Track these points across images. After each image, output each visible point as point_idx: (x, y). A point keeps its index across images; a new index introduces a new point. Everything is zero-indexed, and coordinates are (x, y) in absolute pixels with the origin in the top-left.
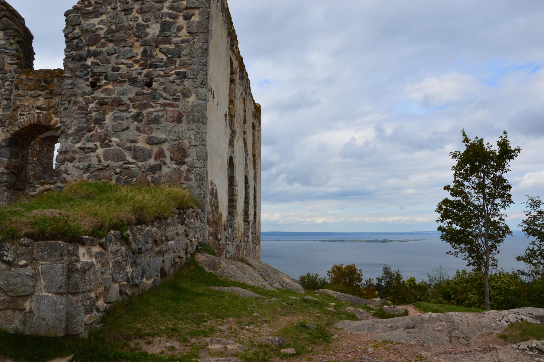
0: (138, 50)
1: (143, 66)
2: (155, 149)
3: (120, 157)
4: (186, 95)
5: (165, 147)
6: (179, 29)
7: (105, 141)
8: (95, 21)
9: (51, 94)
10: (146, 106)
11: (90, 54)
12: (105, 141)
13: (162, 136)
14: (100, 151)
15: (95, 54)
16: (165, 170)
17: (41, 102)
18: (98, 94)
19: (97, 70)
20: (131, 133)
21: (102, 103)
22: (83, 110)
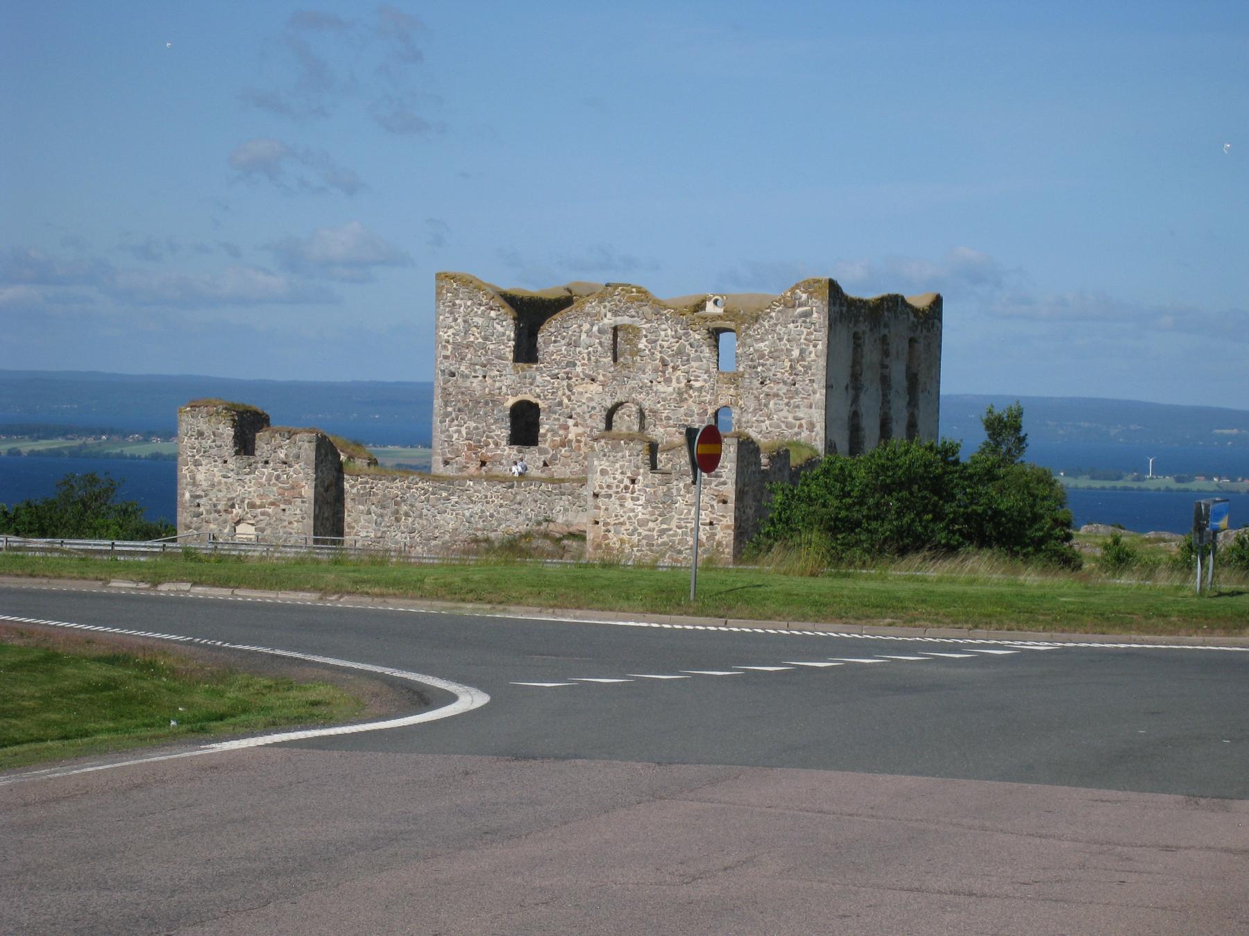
2: (798, 423)
3: (779, 427)
4: (814, 393)
5: (803, 422)
7: (769, 417)
8: (762, 345)
9: (737, 388)
10: (792, 398)
11: (759, 364)
12: (769, 417)
13: (801, 415)
14: (767, 422)
16: (803, 435)
18: (765, 389)
20: (784, 413)
21: (767, 395)
22: (757, 398)
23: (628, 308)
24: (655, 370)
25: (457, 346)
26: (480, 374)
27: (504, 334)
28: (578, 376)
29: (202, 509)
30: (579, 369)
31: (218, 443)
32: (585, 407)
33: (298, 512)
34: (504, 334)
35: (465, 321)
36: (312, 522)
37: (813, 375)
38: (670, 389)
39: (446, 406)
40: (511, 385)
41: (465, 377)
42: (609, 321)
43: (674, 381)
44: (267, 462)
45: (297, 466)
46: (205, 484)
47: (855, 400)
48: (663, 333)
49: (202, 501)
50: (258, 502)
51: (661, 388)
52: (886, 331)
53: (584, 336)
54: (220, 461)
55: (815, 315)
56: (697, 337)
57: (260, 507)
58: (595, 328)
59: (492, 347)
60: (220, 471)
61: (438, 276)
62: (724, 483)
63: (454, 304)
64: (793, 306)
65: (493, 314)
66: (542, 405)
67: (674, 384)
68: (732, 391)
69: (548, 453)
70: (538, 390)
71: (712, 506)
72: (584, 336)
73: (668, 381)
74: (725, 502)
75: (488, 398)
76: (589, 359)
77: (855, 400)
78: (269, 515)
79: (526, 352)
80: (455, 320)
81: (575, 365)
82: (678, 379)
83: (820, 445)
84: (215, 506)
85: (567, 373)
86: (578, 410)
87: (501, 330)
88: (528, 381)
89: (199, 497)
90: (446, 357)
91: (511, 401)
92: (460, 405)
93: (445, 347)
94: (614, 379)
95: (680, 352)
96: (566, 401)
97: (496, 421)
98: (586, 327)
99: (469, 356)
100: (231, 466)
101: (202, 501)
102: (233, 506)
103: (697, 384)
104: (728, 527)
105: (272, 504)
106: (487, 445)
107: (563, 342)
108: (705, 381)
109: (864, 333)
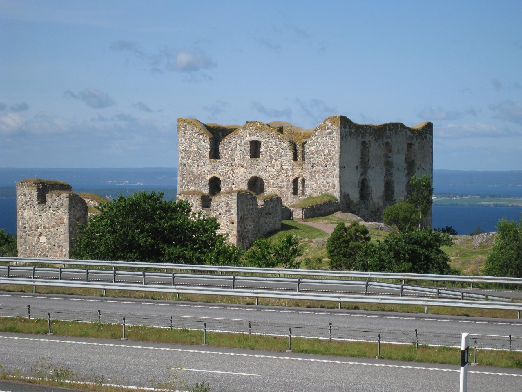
0: (323, 157)
1: (325, 162)
3: (320, 187)
4: (335, 170)
5: (330, 184)
6: (333, 151)
7: (316, 182)
8: (312, 148)
10: (325, 173)
12: (316, 182)
13: (330, 181)
14: (315, 185)
15: (313, 158)
16: (330, 190)
17: (300, 170)
18: (314, 169)
19: (314, 162)
20: (322, 180)
21: (315, 172)
23: (256, 132)
24: (268, 161)
26: (196, 165)
27: (205, 146)
28: (236, 165)
29: (26, 229)
30: (236, 161)
31: (32, 199)
32: (239, 179)
33: (63, 230)
34: (205, 146)
35: (190, 141)
36: (68, 235)
37: (334, 162)
38: (274, 170)
39: (183, 180)
40: (208, 169)
41: (191, 166)
42: (249, 139)
43: (276, 166)
44: (50, 207)
45: (62, 209)
46: (27, 218)
47: (364, 173)
48: (270, 144)
49: (26, 226)
50: (47, 226)
51: (270, 169)
52: (389, 140)
53: (238, 146)
54: (32, 207)
55: (334, 133)
56: (285, 145)
57: (49, 228)
58: (243, 142)
59: (201, 152)
60: (33, 212)
61: (178, 120)
62: (232, 214)
63: (185, 133)
64: (325, 129)
65: (201, 137)
66: (221, 179)
67: (276, 167)
68: (300, 170)
70: (220, 172)
71: (227, 225)
72: (238, 146)
73: (273, 166)
74: (233, 223)
76: (240, 157)
77: (364, 173)
78: (51, 232)
79: (215, 154)
80: (186, 140)
81: (235, 160)
82: (277, 165)
83: (337, 195)
84: (31, 228)
85: (232, 163)
86: (236, 181)
87: (204, 144)
88: (215, 167)
89: (25, 224)
90: (182, 157)
91: (209, 177)
92: (188, 179)
93: (182, 153)
94: (251, 166)
95: (278, 153)
96: (231, 176)
98: (239, 142)
100: (37, 209)
101: (26, 226)
102: (38, 228)
103: (285, 167)
104: (234, 235)
105: (53, 227)
107: (229, 149)
108: (288, 165)
109: (370, 141)
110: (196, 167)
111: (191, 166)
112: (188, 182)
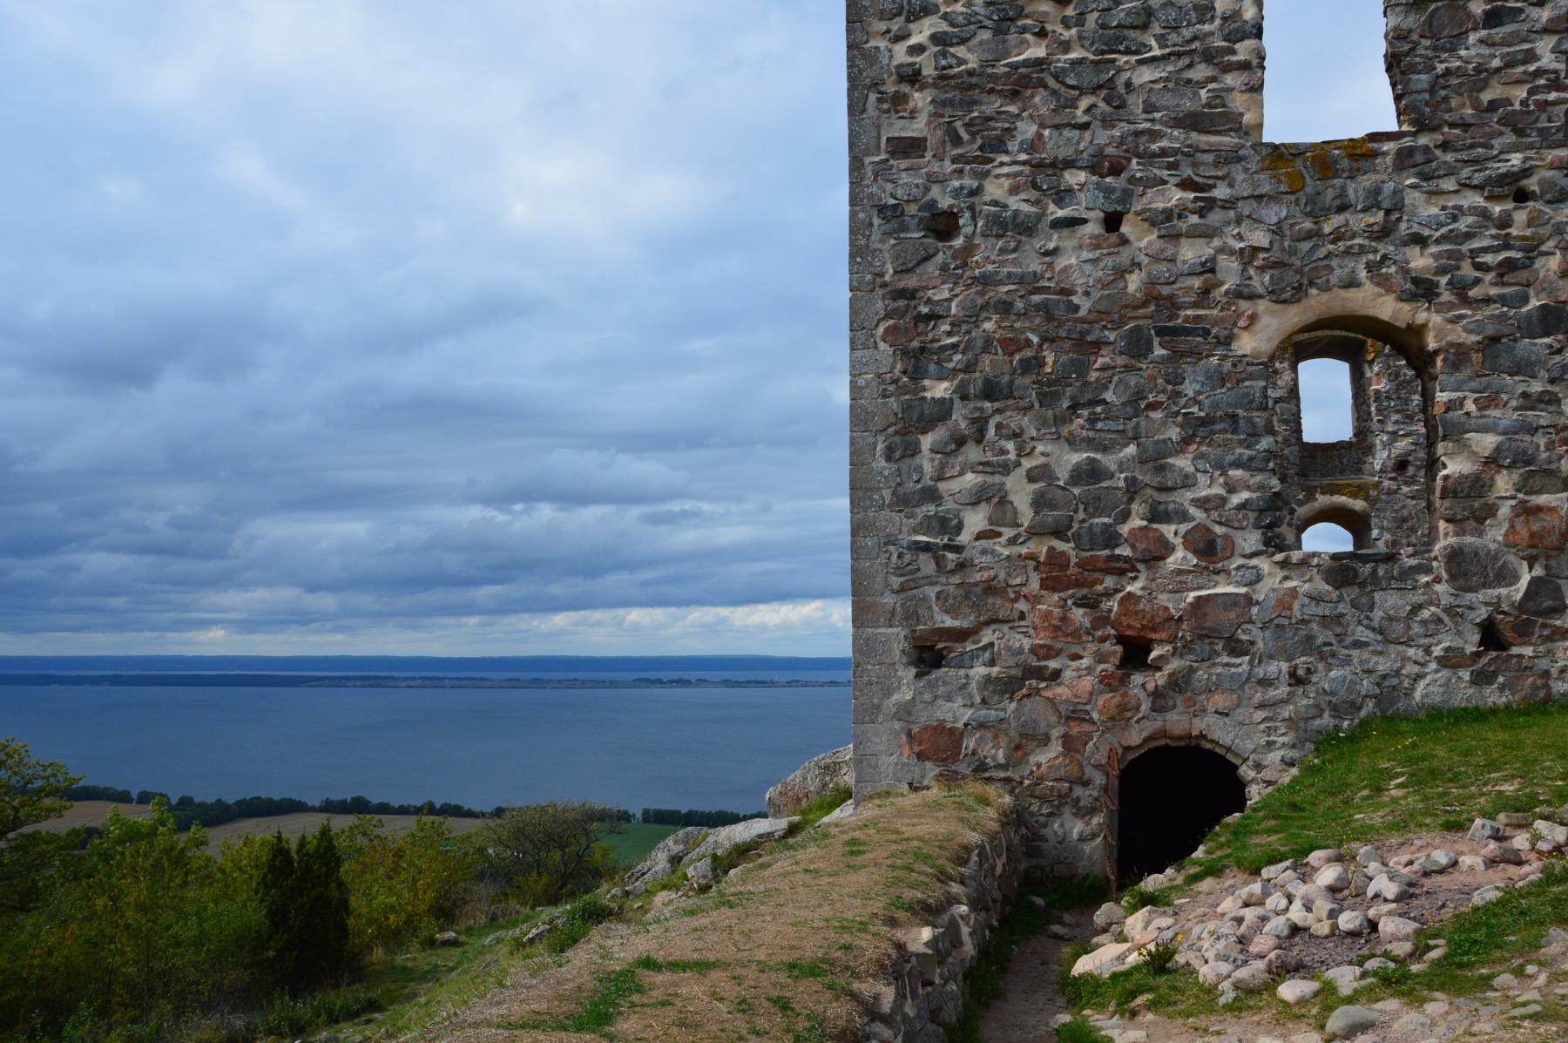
25: (958, 89)
39: (917, 374)
59: (1145, 75)
69: (1506, 576)
70: (1420, 261)
75: (1142, 320)
93: (899, 100)
97: (1197, 429)
99: (1027, 130)
106: (1156, 553)
110: (1093, 228)
111: (1025, 227)
112: (991, 391)
